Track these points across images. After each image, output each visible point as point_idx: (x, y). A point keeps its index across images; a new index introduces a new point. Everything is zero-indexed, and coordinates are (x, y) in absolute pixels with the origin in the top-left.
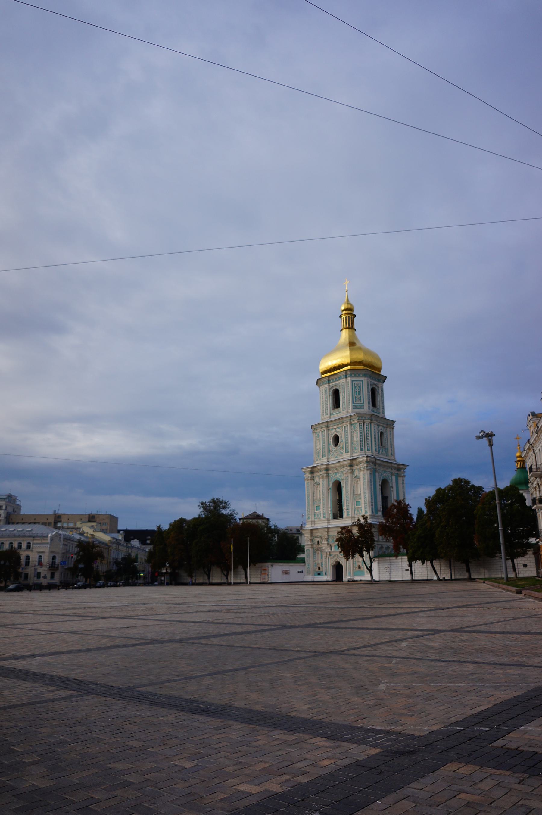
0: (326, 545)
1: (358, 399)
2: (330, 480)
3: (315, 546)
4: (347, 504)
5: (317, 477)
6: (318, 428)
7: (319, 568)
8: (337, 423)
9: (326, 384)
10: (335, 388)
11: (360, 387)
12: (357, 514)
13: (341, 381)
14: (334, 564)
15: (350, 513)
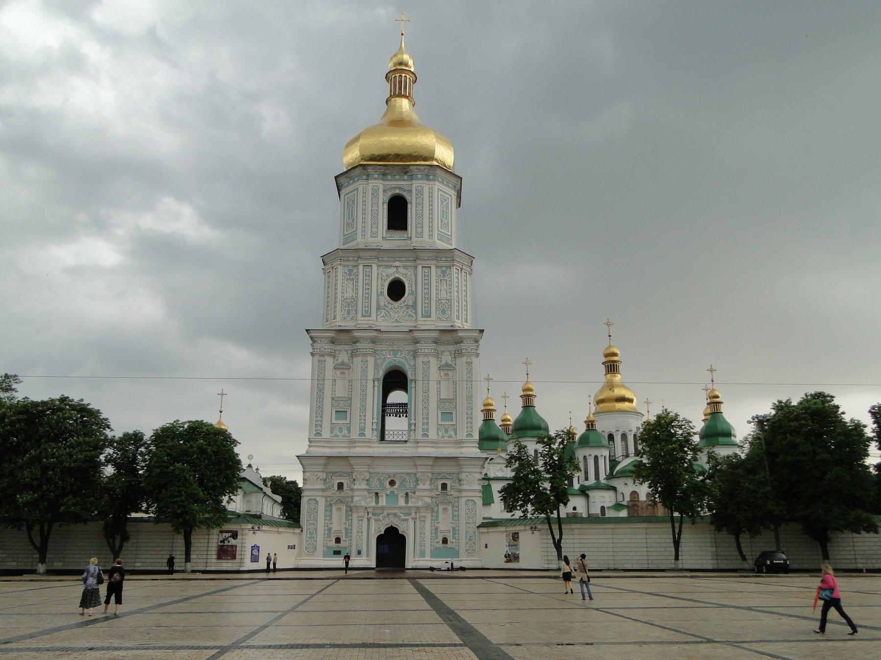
0: (365, 493)
1: (444, 225)
2: (379, 361)
3: (328, 494)
4: (423, 415)
5: (345, 353)
6: (351, 259)
7: (338, 540)
8: (401, 258)
9: (375, 179)
10: (397, 191)
11: (448, 203)
12: (443, 437)
13: (414, 182)
14: (383, 533)
15: (429, 434)
